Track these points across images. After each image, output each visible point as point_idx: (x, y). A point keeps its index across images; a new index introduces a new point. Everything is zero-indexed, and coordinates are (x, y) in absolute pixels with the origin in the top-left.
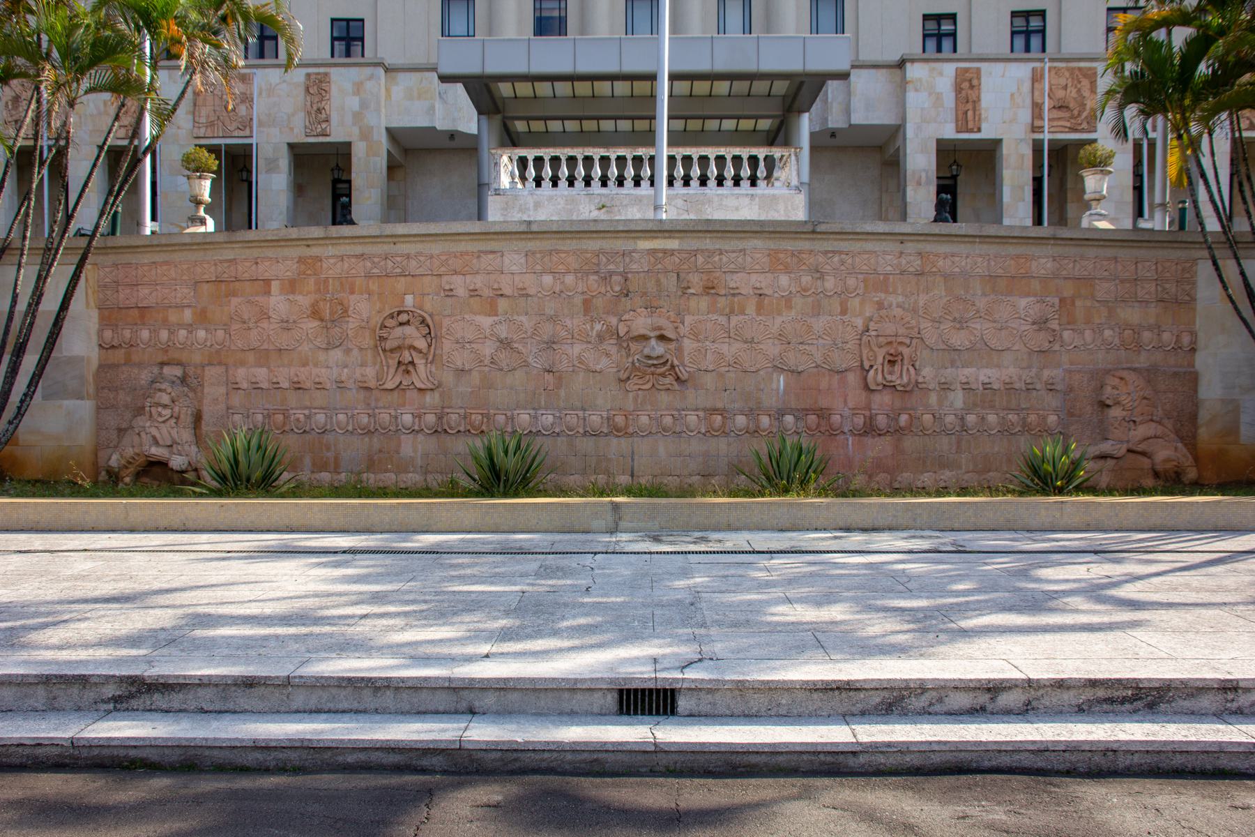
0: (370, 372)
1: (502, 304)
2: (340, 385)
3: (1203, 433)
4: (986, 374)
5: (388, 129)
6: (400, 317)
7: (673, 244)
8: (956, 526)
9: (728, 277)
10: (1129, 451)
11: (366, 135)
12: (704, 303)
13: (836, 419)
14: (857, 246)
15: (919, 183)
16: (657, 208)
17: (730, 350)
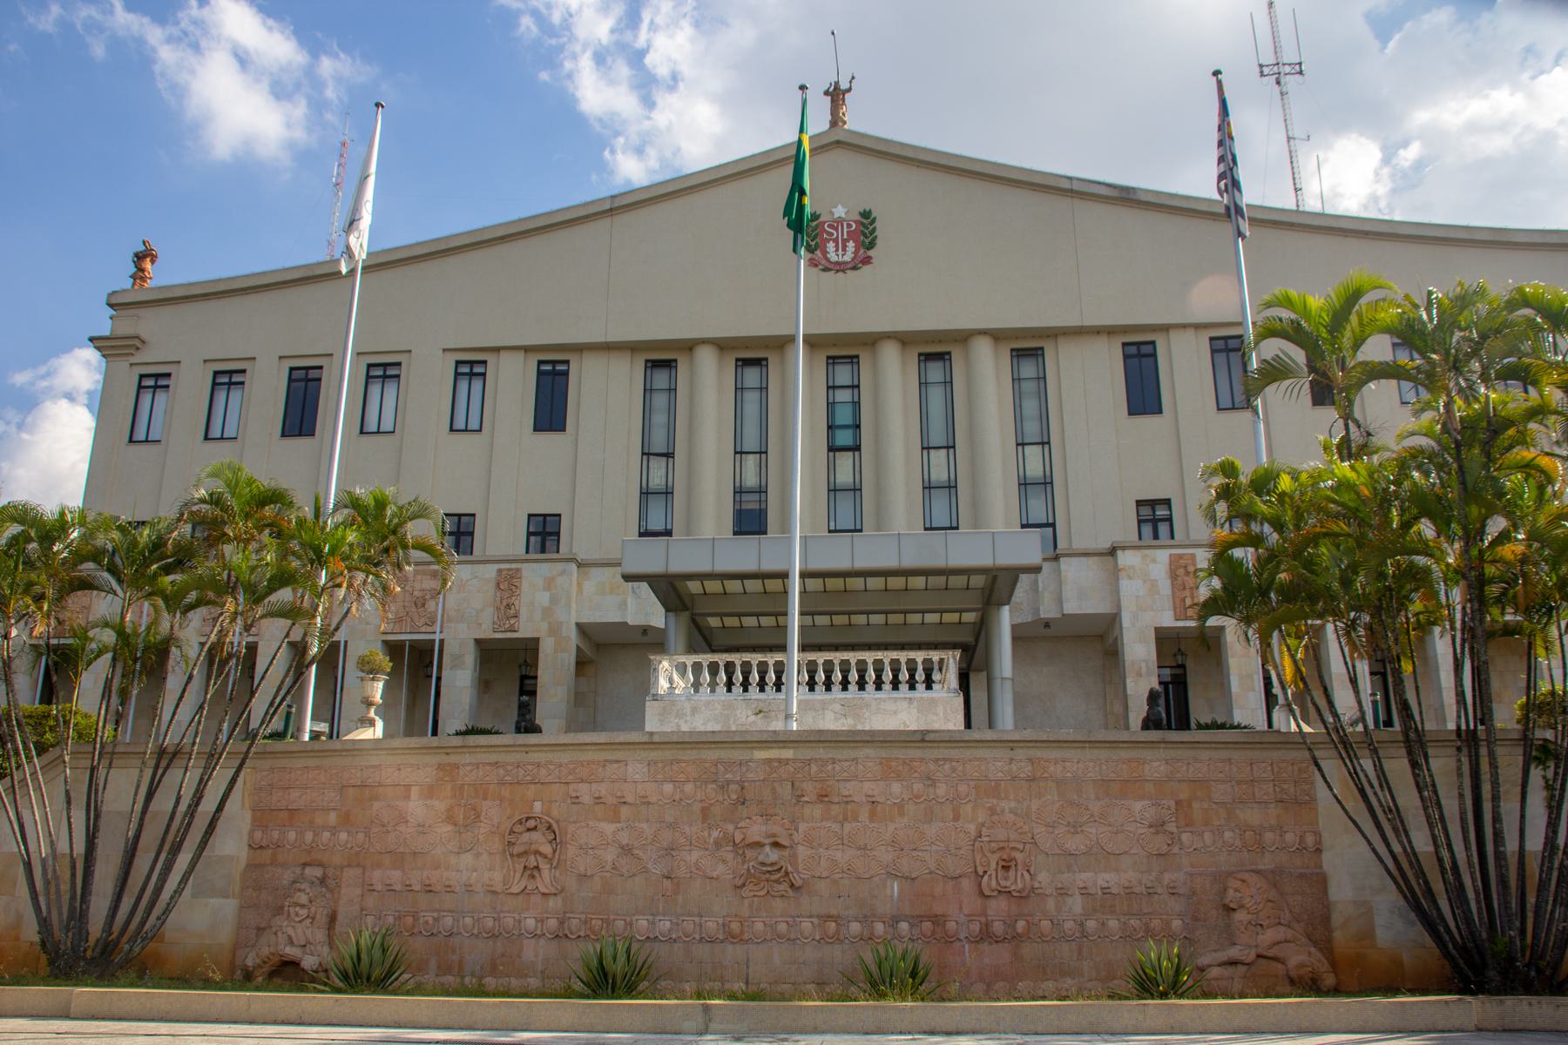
0: (497, 876)
1: (624, 811)
2: (469, 889)
3: (1338, 936)
4: (1105, 879)
5: (578, 625)
6: (528, 823)
7: (788, 754)
8: (1040, 1029)
9: (841, 785)
10: (1258, 956)
11: (554, 630)
12: (818, 811)
13: (951, 926)
14: (968, 753)
15: (1139, 675)
16: (788, 717)
17: (843, 856)
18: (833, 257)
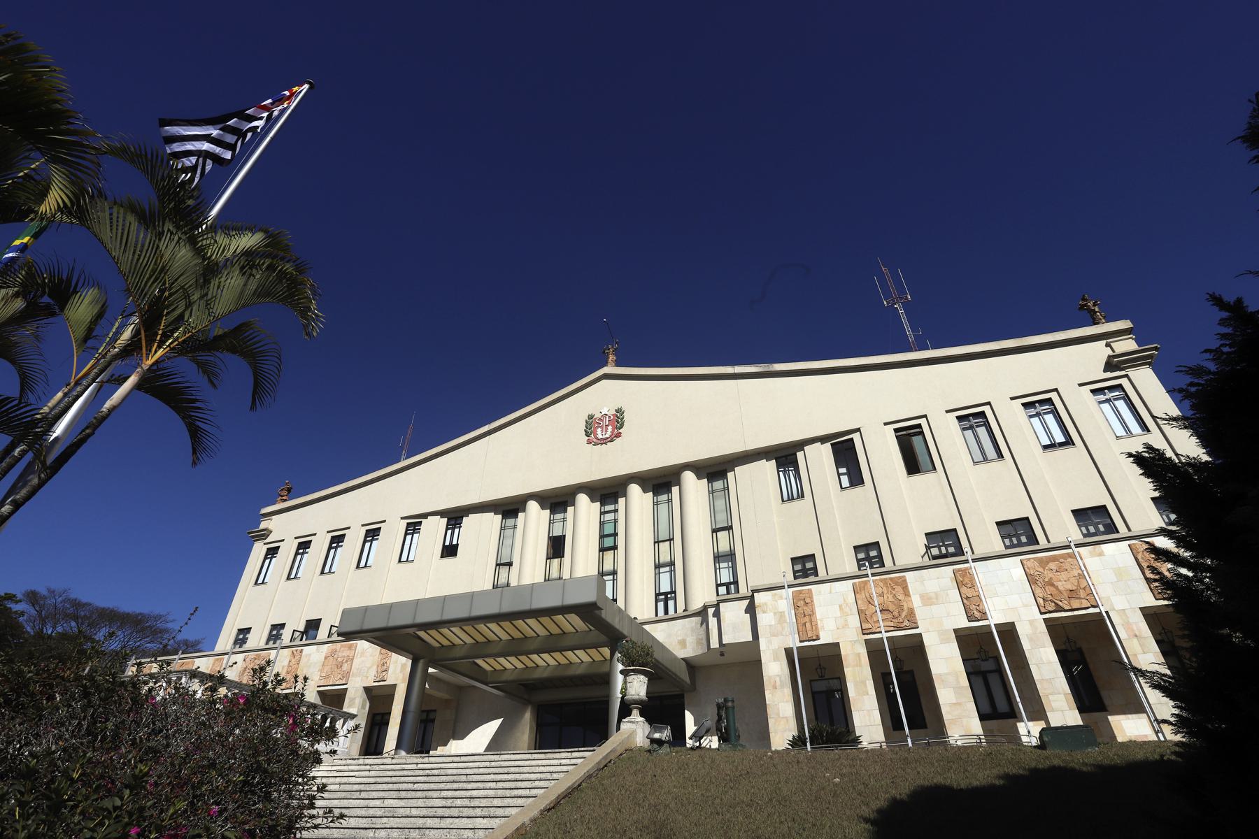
18: (600, 436)
